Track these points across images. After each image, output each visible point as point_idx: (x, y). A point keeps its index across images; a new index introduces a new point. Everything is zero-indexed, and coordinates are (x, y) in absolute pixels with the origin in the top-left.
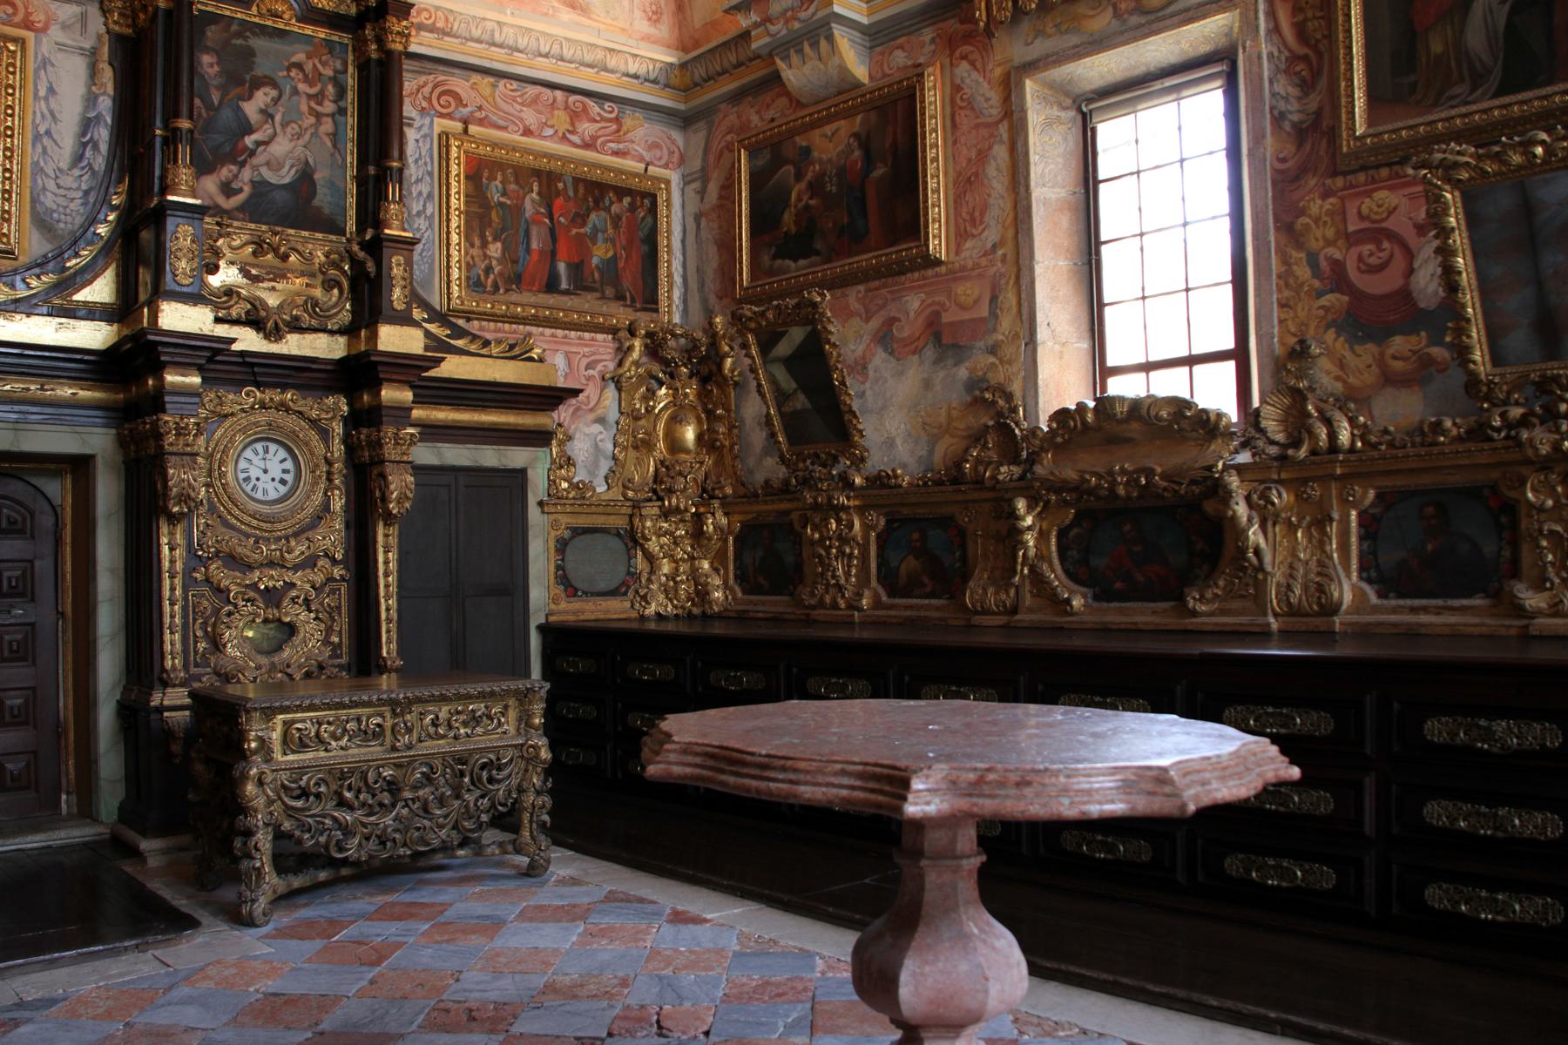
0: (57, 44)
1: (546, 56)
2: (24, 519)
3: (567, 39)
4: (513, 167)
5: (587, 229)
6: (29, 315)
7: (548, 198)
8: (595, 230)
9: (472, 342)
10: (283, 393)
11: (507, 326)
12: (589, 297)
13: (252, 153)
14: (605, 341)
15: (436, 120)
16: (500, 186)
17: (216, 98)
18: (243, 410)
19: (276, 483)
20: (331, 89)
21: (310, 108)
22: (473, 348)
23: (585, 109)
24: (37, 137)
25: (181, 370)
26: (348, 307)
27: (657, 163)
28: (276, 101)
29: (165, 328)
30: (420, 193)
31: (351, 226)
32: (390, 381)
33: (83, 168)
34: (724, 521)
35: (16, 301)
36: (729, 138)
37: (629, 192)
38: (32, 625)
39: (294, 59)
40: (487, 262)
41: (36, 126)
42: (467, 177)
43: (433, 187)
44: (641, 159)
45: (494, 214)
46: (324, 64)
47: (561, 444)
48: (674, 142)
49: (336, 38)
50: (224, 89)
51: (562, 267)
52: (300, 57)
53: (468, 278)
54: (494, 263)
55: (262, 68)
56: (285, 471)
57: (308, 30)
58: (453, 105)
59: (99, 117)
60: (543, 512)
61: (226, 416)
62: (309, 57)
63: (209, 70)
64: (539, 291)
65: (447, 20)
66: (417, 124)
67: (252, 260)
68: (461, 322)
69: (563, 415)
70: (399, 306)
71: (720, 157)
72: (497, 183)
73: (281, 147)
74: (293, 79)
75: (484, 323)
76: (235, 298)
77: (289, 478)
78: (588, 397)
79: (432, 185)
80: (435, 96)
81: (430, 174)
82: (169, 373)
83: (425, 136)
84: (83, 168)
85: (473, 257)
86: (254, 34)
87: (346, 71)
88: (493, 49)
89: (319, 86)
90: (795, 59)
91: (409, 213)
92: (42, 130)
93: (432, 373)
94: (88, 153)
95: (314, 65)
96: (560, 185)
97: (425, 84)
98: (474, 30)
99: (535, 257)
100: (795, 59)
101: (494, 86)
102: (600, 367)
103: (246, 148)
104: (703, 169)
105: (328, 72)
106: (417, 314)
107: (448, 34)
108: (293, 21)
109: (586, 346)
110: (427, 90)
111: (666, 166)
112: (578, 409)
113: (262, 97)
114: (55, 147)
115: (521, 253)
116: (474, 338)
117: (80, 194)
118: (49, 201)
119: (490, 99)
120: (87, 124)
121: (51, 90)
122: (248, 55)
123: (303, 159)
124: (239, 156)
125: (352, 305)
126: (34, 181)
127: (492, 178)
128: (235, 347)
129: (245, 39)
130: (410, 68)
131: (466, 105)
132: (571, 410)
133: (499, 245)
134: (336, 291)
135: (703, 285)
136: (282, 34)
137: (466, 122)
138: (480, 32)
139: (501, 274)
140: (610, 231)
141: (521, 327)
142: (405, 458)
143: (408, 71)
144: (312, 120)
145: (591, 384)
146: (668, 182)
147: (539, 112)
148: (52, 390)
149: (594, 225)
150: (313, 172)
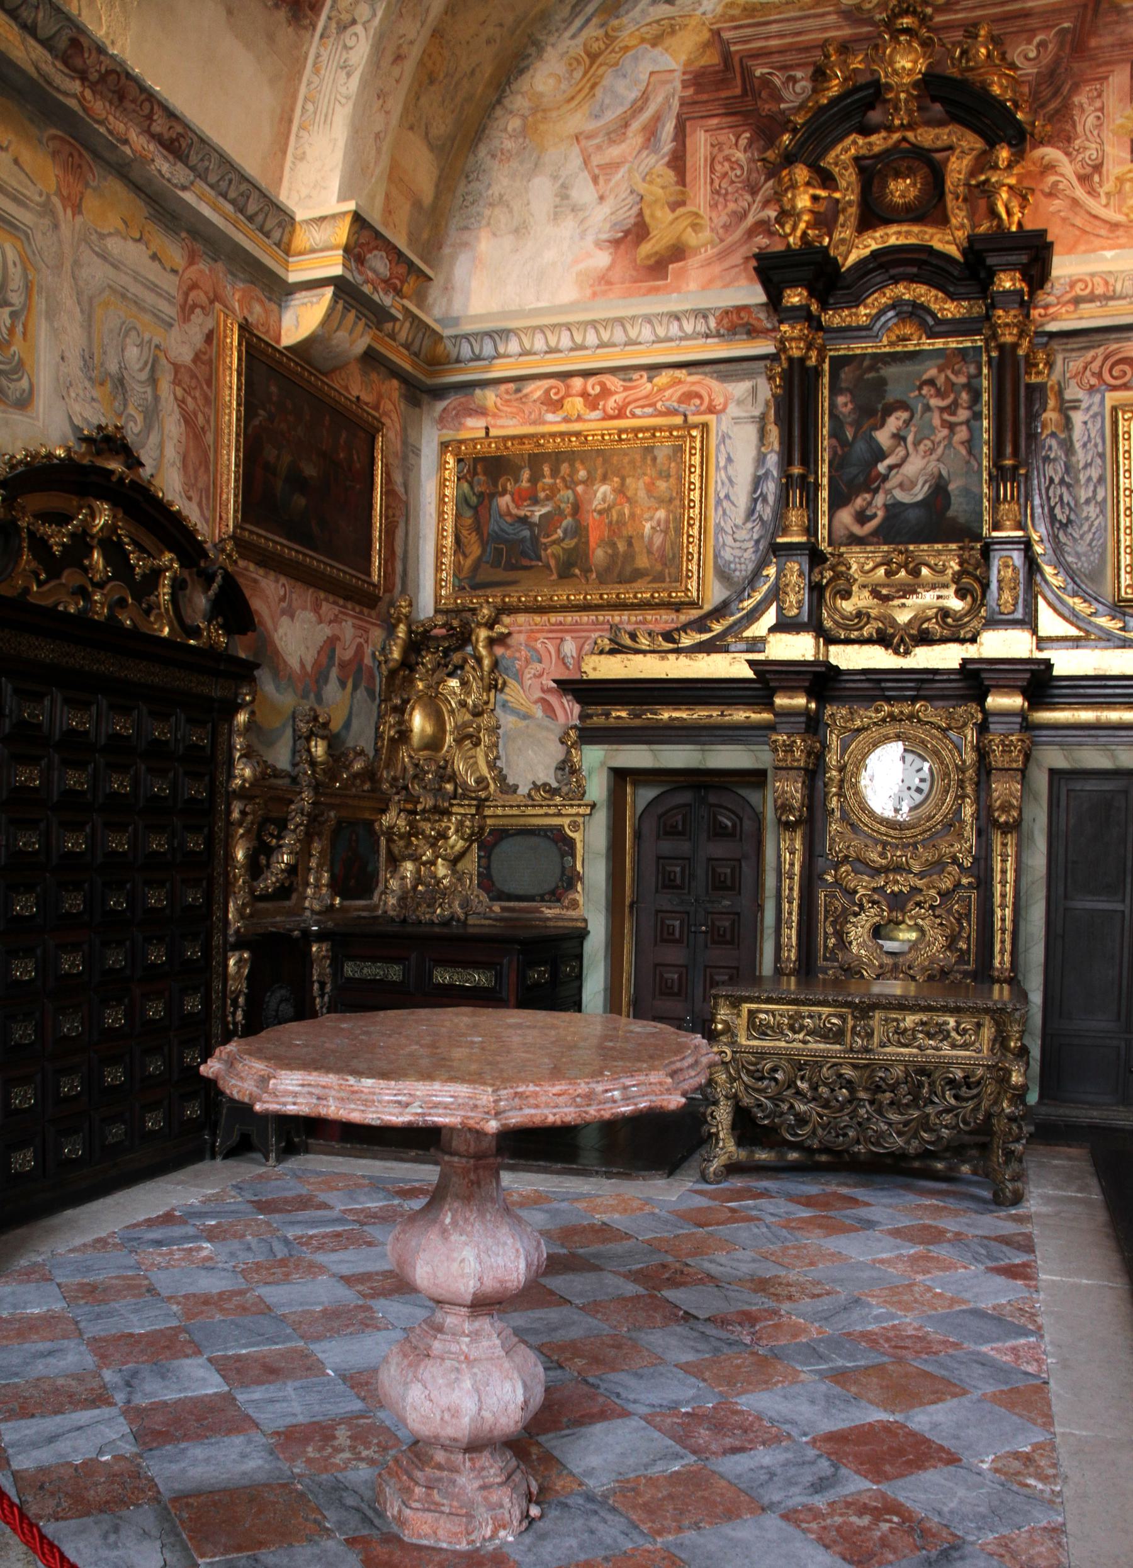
2: (734, 825)
6: (709, 653)
10: (913, 704)
13: (885, 478)
15: (1107, 394)
18: (875, 724)
20: (964, 396)
21: (943, 421)
24: (719, 502)
28: (907, 423)
35: (701, 643)
38: (738, 914)
39: (925, 377)
46: (956, 373)
50: (857, 425)
52: (933, 372)
55: (893, 393)
56: (922, 780)
57: (939, 343)
61: (859, 730)
62: (941, 369)
65: (1107, 283)
66: (1084, 405)
67: (884, 579)
73: (915, 466)
77: (925, 786)
79: (1104, 468)
81: (1102, 456)
83: (1094, 416)
86: (886, 363)
89: (952, 396)
92: (722, 495)
94: (759, 506)
95: (947, 377)
97: (1094, 358)
103: (879, 474)
105: (962, 380)
107: (1112, 298)
108: (924, 340)
110: (1095, 366)
113: (894, 422)
118: (727, 554)
120: (757, 481)
121: (729, 460)
122: (882, 382)
123: (936, 471)
124: (871, 483)
126: (717, 539)
134: (969, 599)
142: (1014, 765)
144: (945, 432)
150: (947, 483)
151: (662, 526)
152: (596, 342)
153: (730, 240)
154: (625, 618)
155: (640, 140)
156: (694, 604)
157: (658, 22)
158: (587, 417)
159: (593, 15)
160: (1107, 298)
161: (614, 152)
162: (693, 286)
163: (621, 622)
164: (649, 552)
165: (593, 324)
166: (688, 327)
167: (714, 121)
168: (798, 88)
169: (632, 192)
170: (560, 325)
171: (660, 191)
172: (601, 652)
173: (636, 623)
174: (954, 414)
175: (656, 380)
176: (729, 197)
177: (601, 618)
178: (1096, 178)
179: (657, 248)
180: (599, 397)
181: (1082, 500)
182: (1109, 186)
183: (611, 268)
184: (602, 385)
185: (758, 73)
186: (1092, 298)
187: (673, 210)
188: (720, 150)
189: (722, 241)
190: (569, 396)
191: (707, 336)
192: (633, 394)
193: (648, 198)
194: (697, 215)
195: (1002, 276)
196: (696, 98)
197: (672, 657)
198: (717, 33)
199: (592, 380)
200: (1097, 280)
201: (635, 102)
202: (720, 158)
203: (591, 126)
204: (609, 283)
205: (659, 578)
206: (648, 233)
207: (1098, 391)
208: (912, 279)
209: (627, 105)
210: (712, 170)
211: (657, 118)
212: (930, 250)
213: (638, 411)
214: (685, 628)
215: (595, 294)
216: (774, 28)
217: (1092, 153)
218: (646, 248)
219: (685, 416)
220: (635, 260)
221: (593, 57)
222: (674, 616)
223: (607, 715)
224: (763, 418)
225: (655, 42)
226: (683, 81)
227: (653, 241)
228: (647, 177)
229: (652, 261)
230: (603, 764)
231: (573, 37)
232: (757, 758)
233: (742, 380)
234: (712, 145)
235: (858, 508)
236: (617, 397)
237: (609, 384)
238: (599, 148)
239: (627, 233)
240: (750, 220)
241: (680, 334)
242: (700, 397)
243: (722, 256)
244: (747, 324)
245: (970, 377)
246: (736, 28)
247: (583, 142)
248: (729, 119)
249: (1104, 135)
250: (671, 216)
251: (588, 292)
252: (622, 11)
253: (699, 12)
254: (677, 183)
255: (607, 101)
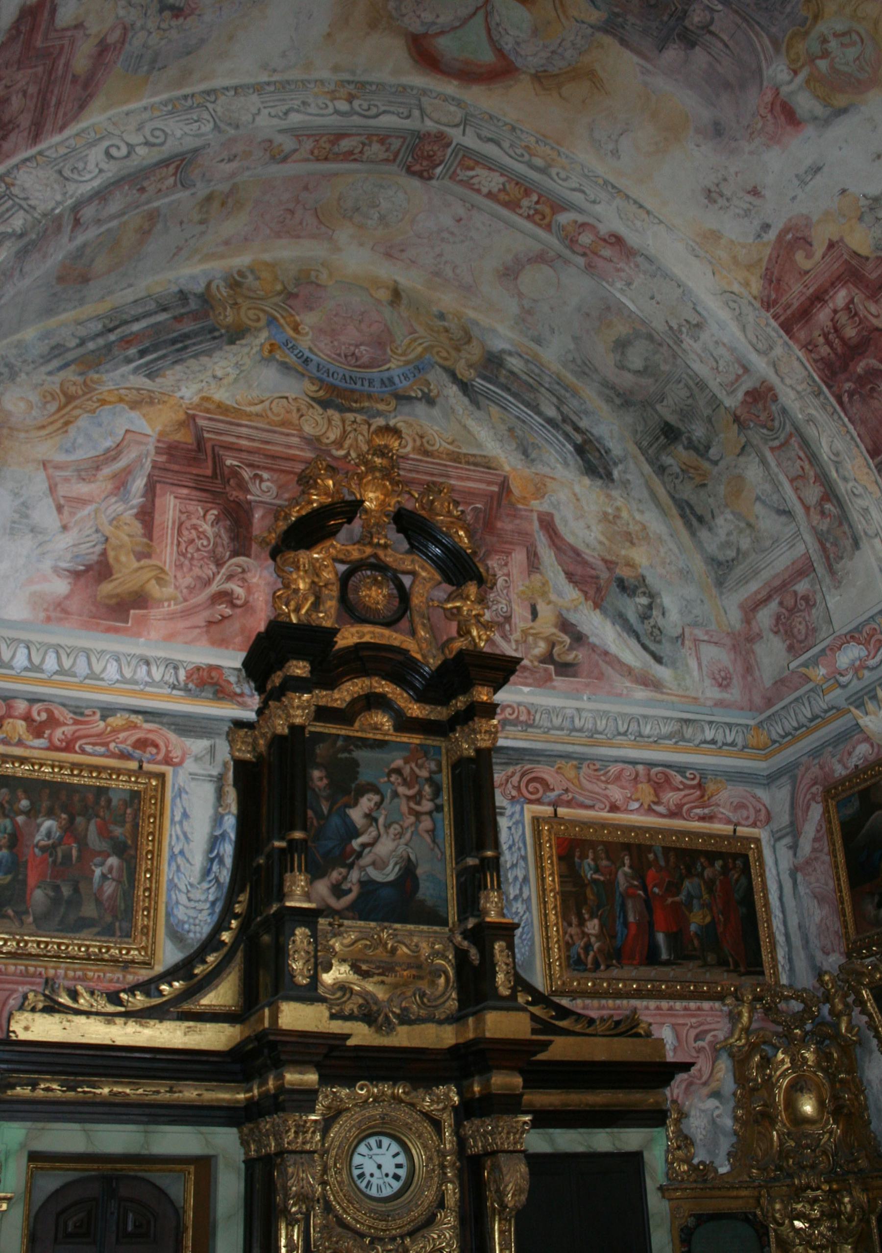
0: (190, 774)
1: (625, 734)
3: (645, 717)
4: (603, 843)
5: (682, 897)
6: (161, 1020)
7: (639, 871)
8: (690, 897)
9: (577, 1021)
10: (394, 1085)
11: (610, 1002)
12: (691, 965)
13: (359, 855)
14: (712, 1009)
15: (526, 806)
16: (592, 863)
17: (325, 808)
19: (390, 1180)
20: (427, 789)
21: (410, 809)
22: (578, 1028)
23: (668, 780)
24: (173, 857)
25: (298, 1068)
26: (454, 995)
27: (743, 822)
28: (378, 805)
29: (284, 1027)
30: (516, 878)
31: (452, 915)
32: (499, 1068)
33: (210, 881)
34: (864, 1198)
36: (814, 790)
37: (719, 855)
39: (393, 765)
40: (585, 939)
41: (171, 848)
42: (560, 858)
43: (527, 871)
44: (729, 821)
45: (588, 891)
46: (420, 767)
47: (678, 1121)
48: (759, 800)
49: (429, 742)
51: (660, 937)
52: (399, 763)
53: (568, 958)
54: (593, 939)
55: (365, 776)
56: (399, 1166)
57: (404, 738)
58: (541, 791)
59: (223, 836)
60: (663, 1197)
62: (407, 761)
63: (319, 783)
64: (641, 964)
65: (529, 713)
66: (508, 812)
68: (565, 1002)
69: (676, 1091)
70: (504, 991)
71: (808, 808)
72: (589, 860)
73: (385, 847)
74: (393, 783)
75: (588, 1001)
76: (348, 995)
77: (402, 1172)
78: (700, 1070)
80: (523, 785)
81: (525, 858)
82: (287, 1072)
83: (516, 823)
84: (210, 881)
85: (571, 936)
86: (357, 747)
87: (440, 771)
88: (574, 734)
90: (871, 706)
91: (507, 898)
92: (176, 850)
93: (541, 1057)
94: (215, 867)
95: (411, 768)
96: (651, 856)
97: (513, 774)
98: (554, 719)
99: (633, 930)
100: (871, 706)
101: (579, 768)
102: (709, 1038)
103: (354, 850)
104: (792, 824)
105: (424, 774)
106: (521, 999)
107: (531, 726)
109: (693, 1016)
111: (754, 825)
112: (691, 1084)
113: (367, 802)
114: (188, 865)
115: (619, 928)
116: (579, 1017)
117: (208, 905)
118: (180, 913)
119: (576, 781)
120: (214, 841)
121: (185, 815)
123: (405, 854)
125: (458, 994)
127: (584, 856)
128: (350, 1042)
129: (350, 751)
130: (498, 761)
131: (553, 790)
132: (683, 1086)
133: (596, 921)
135: (807, 942)
136: (381, 745)
137: (555, 804)
138: (560, 720)
139: (600, 950)
140: (706, 896)
141: (625, 1002)
143: (497, 764)
144: (412, 819)
145: (702, 1056)
146: (757, 841)
147: (623, 788)
148: (180, 1092)
149: (689, 893)
150: (415, 867)
151: (115, 873)
152: (56, 667)
153: (193, 601)
154: (61, 972)
155: (110, 486)
156: (147, 964)
157: (138, 389)
158: (31, 743)
159: (73, 361)
160: (529, 725)
161: (83, 489)
162: (153, 634)
163: (56, 976)
164: (98, 902)
165: (57, 649)
166: (157, 674)
167: (185, 491)
168: (264, 485)
169: (97, 531)
170: (19, 641)
171: (126, 538)
172: (33, 1010)
173: (74, 979)
174: (418, 803)
175: (110, 720)
176: (195, 562)
177: (31, 969)
178: (507, 627)
179: (119, 590)
180: (43, 725)
181: (512, 897)
182: (516, 635)
183: (67, 597)
184: (50, 712)
185: (229, 462)
186: (516, 723)
187: (139, 560)
188: (189, 518)
189: (185, 600)
190: (11, 717)
191: (174, 687)
192: (83, 729)
193: (113, 541)
194: (162, 570)
195: (480, 688)
196: (168, 466)
197: (119, 1021)
198: (193, 417)
199: (36, 707)
200: (522, 708)
201: (108, 450)
202: (188, 524)
203: (61, 457)
204: (65, 611)
205: (108, 931)
206: (111, 574)
207: (518, 802)
208: (365, 672)
209: (100, 451)
210: (180, 533)
211: (128, 471)
212: (405, 652)
213: (88, 748)
214: (131, 990)
215: (48, 619)
216: (244, 430)
217: (503, 606)
218: (107, 588)
219: (141, 762)
220: (95, 596)
221: (70, 398)
222: (120, 975)
223: (34, 1085)
224: (221, 778)
225: (134, 405)
226: (156, 447)
227: (117, 582)
228: (115, 521)
229: (113, 601)
230: (23, 1146)
231: (50, 373)
232: (207, 1142)
233: (201, 737)
234: (181, 511)
235: (334, 882)
236: (65, 729)
237: (56, 712)
238: (67, 480)
239: (89, 568)
240: (214, 588)
241: (147, 679)
242: (156, 746)
243: (187, 613)
244: (216, 684)
245: (431, 772)
246: (210, 419)
247: (50, 471)
248: (198, 494)
249: (514, 597)
250: (136, 565)
251: (42, 615)
252: (102, 368)
253: (179, 394)
254: (144, 535)
255: (80, 440)
